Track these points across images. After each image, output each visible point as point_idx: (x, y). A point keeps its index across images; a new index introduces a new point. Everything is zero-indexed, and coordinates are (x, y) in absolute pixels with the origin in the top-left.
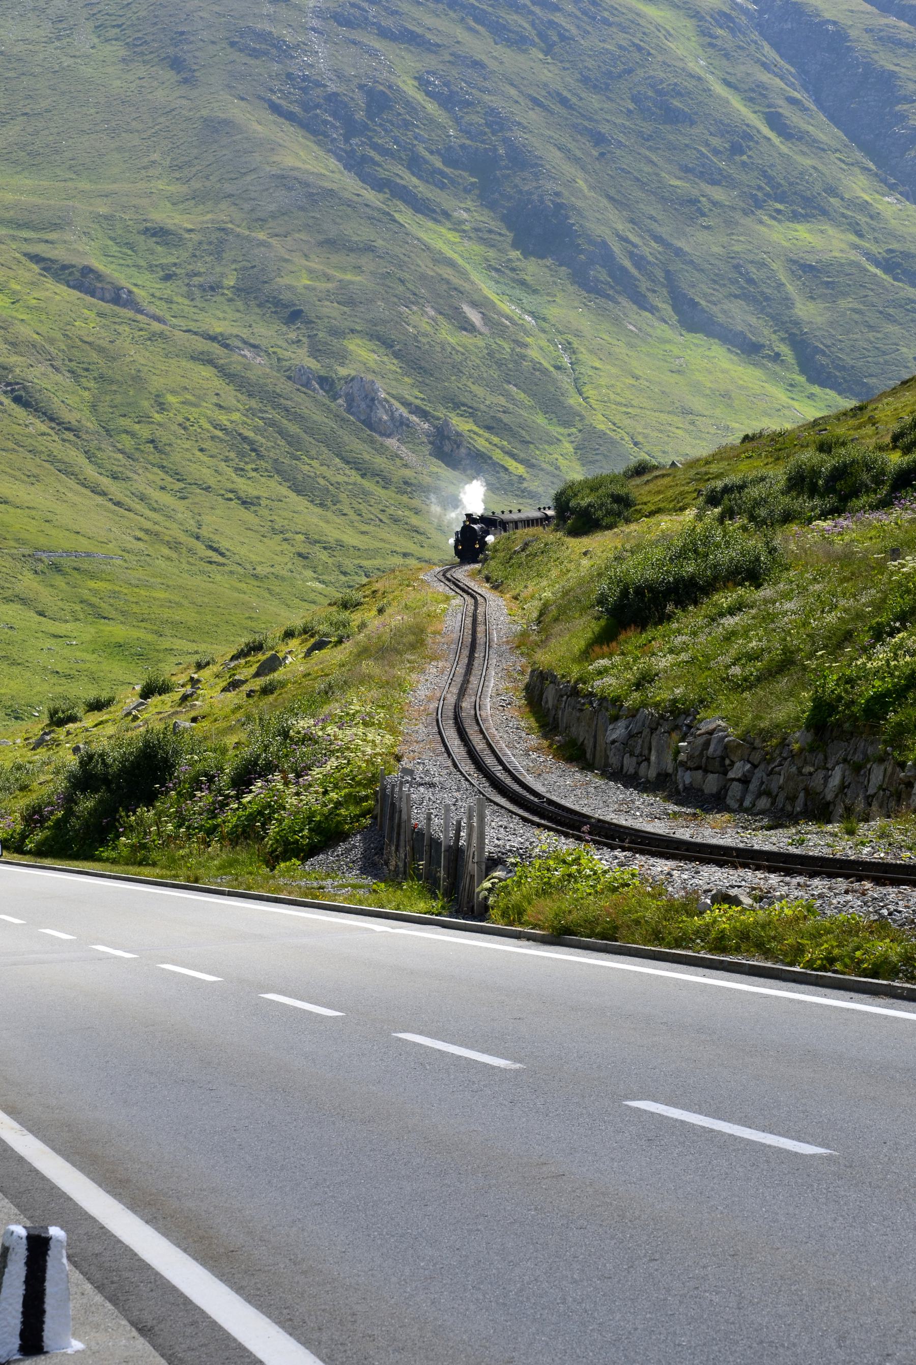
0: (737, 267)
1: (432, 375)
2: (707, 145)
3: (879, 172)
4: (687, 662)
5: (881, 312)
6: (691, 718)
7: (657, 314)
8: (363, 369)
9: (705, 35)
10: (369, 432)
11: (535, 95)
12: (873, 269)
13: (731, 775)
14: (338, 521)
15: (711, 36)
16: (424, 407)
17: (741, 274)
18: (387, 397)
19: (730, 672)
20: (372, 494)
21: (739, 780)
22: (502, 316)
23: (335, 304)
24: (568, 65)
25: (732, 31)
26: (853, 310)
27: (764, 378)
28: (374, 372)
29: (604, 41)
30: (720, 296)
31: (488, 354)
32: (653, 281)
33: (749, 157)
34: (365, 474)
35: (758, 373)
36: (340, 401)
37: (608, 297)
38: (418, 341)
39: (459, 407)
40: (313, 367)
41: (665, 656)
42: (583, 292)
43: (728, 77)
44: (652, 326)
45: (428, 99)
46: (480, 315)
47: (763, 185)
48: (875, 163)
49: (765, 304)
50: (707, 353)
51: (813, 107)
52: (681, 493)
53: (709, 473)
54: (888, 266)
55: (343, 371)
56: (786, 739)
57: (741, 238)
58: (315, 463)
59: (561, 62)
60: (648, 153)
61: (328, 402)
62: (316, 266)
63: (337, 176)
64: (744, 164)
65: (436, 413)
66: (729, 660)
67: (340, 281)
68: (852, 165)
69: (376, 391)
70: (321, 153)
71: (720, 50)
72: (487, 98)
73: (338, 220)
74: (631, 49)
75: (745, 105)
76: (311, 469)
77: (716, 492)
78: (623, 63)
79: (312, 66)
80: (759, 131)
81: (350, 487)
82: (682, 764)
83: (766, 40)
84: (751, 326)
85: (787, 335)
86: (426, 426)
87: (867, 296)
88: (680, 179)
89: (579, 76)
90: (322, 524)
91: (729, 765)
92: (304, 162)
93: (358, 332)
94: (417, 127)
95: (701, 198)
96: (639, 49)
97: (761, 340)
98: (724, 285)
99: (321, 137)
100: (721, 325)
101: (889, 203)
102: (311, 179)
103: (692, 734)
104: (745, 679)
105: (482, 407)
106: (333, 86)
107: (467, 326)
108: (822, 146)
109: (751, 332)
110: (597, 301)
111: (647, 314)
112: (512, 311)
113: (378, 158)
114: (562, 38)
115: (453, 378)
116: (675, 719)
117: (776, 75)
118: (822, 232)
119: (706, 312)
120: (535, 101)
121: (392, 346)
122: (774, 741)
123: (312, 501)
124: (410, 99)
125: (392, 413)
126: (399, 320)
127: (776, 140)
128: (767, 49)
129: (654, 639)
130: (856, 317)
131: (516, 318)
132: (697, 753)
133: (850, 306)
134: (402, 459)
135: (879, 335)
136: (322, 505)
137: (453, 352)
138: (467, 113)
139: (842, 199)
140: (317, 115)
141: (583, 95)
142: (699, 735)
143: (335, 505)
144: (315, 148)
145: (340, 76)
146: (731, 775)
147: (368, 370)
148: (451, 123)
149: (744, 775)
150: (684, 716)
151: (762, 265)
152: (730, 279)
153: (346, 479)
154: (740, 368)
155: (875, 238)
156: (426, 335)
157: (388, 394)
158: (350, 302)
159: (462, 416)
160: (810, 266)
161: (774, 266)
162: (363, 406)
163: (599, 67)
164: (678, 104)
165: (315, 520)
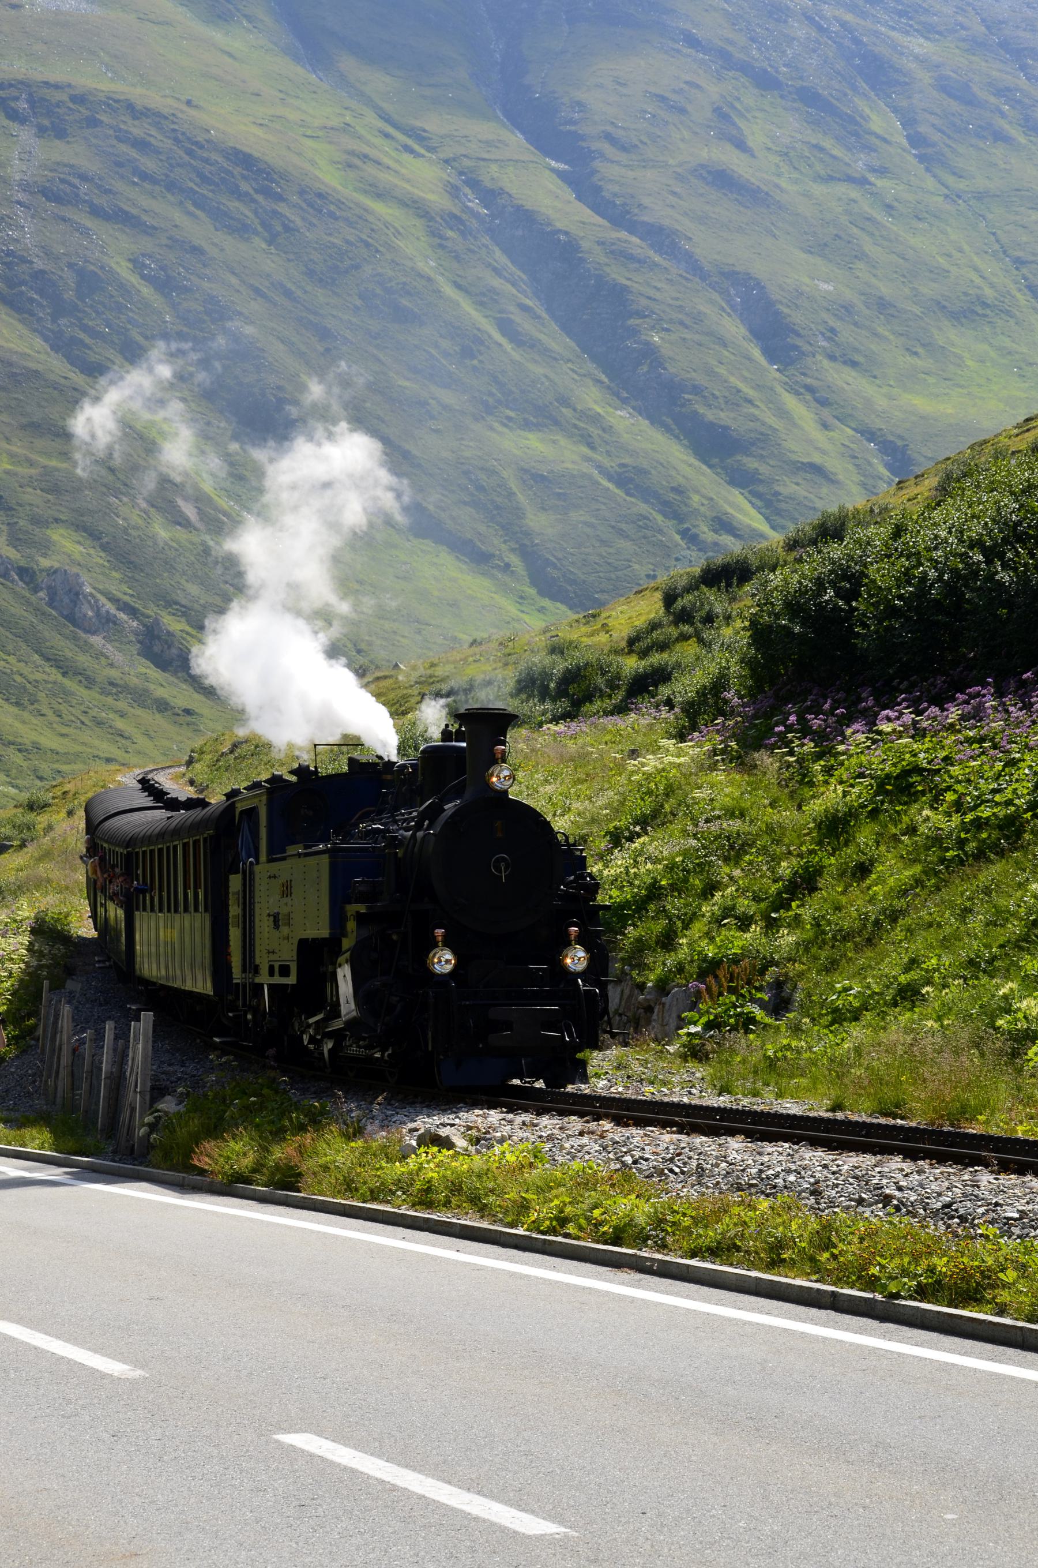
0: (466, 473)
1: (142, 571)
2: (437, 346)
3: (612, 385)
5: (613, 527)
8: (68, 561)
9: (434, 236)
10: (72, 628)
11: (257, 285)
12: (605, 483)
14: (35, 722)
15: (441, 237)
17: (470, 480)
18: (93, 591)
20: (73, 694)
23: (39, 491)
24: (292, 257)
25: (463, 233)
26: (585, 523)
27: (494, 589)
28: (79, 565)
29: (330, 234)
33: (481, 362)
34: (67, 673)
35: (487, 583)
36: (41, 594)
38: (128, 534)
39: (171, 606)
40: (12, 556)
43: (458, 280)
45: (143, 282)
47: (494, 391)
48: (607, 376)
49: (495, 512)
50: (435, 560)
51: (544, 315)
54: (622, 480)
55: (45, 563)
57: (471, 444)
58: (12, 659)
59: (285, 253)
60: (375, 352)
61: (28, 595)
62: (18, 450)
63: (43, 357)
64: (475, 369)
65: (146, 611)
67: (44, 467)
68: (585, 376)
70: (26, 332)
71: (450, 252)
72: (206, 285)
73: (43, 403)
74: (358, 244)
75: (476, 310)
76: (7, 666)
78: (350, 259)
79: (17, 241)
80: (490, 337)
81: (50, 686)
83: (498, 245)
85: (517, 546)
86: (135, 624)
87: (598, 510)
88: (408, 379)
89: (304, 269)
90: (17, 724)
92: (8, 341)
93: (63, 521)
94: (131, 310)
95: (430, 401)
96: (367, 245)
99: (26, 316)
101: (621, 417)
102: (14, 358)
105: (196, 606)
106: (40, 263)
107: (182, 522)
108: (553, 355)
112: (231, 507)
113: (88, 340)
114: (287, 229)
115: (165, 575)
117: (508, 281)
118: (554, 442)
120: (257, 291)
121: (99, 539)
123: (7, 700)
124: (124, 282)
125: (98, 609)
127: (508, 346)
128: (498, 253)
130: (588, 530)
131: (234, 515)
133: (582, 519)
134: (107, 657)
135: (611, 550)
136: (17, 704)
138: (185, 299)
139: (575, 410)
140: (22, 293)
141: (309, 288)
143: (32, 704)
144: (20, 326)
145: (47, 253)
148: (167, 309)
151: (492, 472)
152: (459, 485)
153: (46, 677)
154: (469, 578)
155: (607, 451)
156: (136, 528)
157: (94, 588)
158: (55, 489)
159: (174, 614)
160: (542, 476)
161: (505, 474)
162: (66, 600)
163: (325, 261)
164: (407, 304)
165: (10, 721)
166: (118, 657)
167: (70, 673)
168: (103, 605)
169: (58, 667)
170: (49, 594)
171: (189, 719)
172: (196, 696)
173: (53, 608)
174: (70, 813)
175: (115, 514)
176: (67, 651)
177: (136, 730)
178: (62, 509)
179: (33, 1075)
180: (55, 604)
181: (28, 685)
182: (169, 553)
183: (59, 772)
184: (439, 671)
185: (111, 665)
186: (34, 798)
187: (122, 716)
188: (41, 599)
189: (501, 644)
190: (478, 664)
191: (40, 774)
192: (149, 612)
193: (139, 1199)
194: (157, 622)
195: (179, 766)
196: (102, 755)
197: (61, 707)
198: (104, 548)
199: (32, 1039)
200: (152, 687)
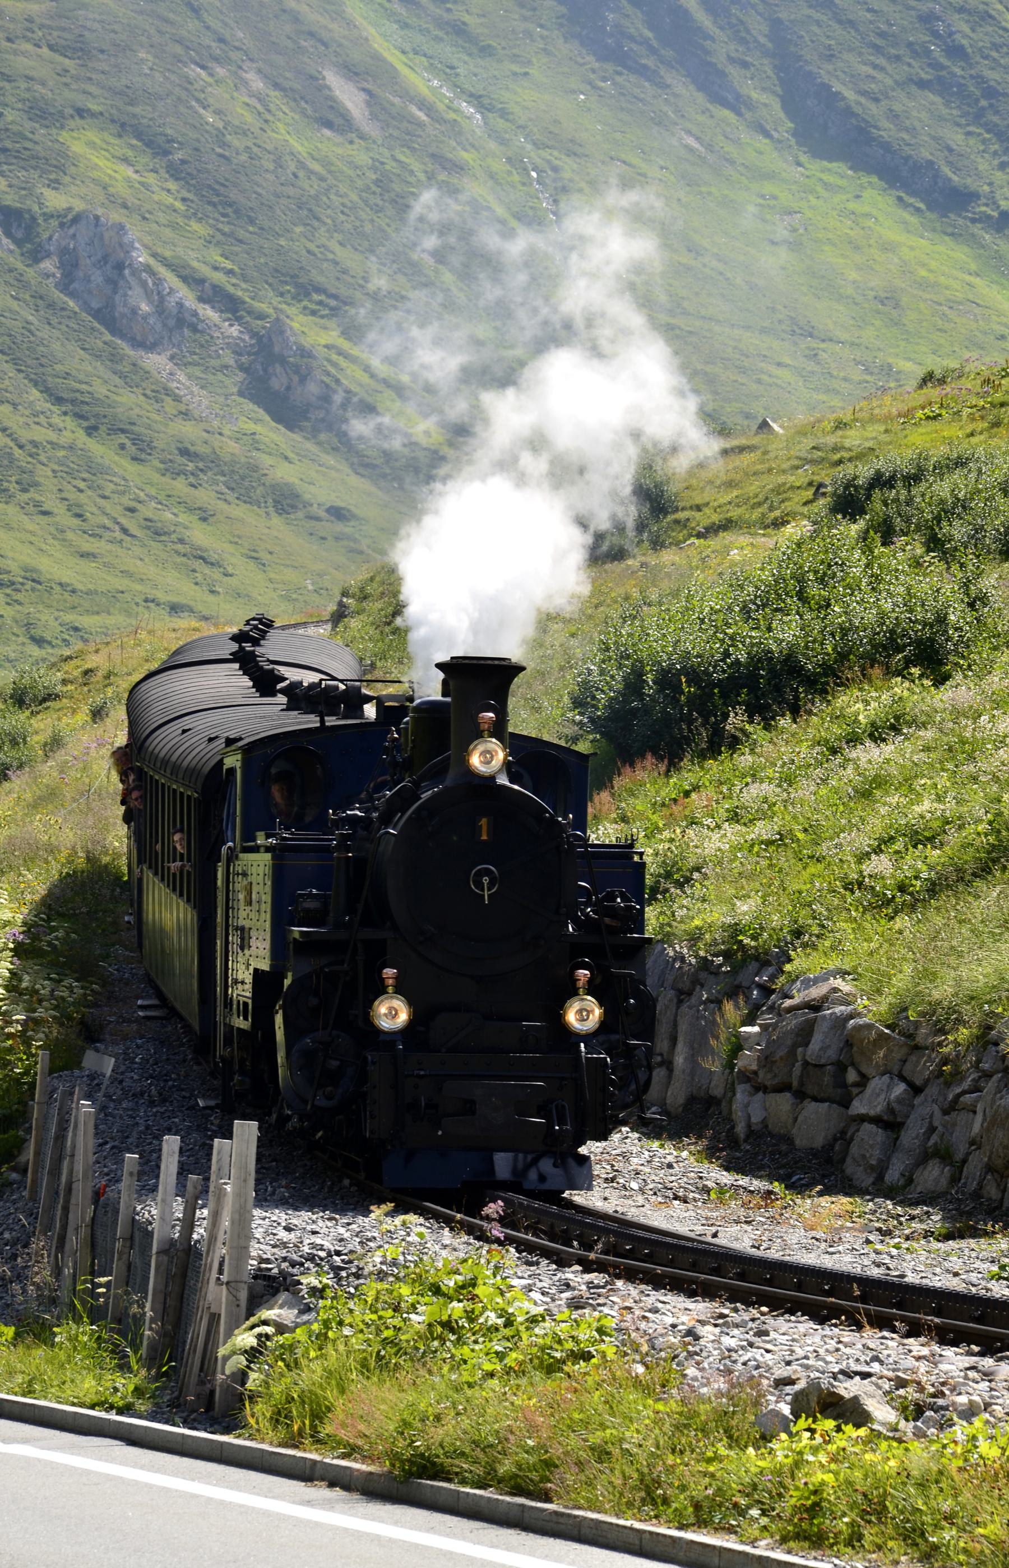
1: (252, 221)
4: (769, 843)
6: (771, 970)
7: (748, 115)
10: (108, 337)
13: (859, 1107)
16: (231, 289)
17: (935, 34)
18: (152, 261)
19: (868, 868)
21: (876, 1120)
22: (412, 100)
27: (973, 267)
28: (125, 206)
30: (889, 82)
31: (377, 182)
32: (743, 41)
34: (95, 428)
35: (962, 253)
37: (643, 71)
38: (224, 145)
41: (718, 827)
42: (590, 58)
44: (737, 142)
46: (363, 96)
49: (984, 103)
52: (778, 490)
53: (843, 448)
56: (990, 1028)
65: (256, 304)
66: (865, 842)
69: (127, 248)
77: (856, 487)
81: (61, 453)
82: (746, 1077)
84: (951, 150)
86: (234, 331)
91: (857, 1085)
97: (972, 184)
98: (898, 58)
100: (886, 147)
103: (771, 1009)
104: (902, 888)
109: (950, 164)
110: (619, 79)
111: (726, 113)
115: (298, 230)
116: (734, 972)
119: (855, 115)
121: (166, 153)
122: (964, 1033)
125: (162, 299)
126: (184, 95)
129: (696, 788)
131: (441, 107)
132: (781, 1053)
134: (177, 399)
137: (301, 174)
142: (791, 1009)
143: (25, 490)
146: (859, 1107)
147: (112, 200)
149: (890, 1110)
150: (754, 966)
152: (910, 45)
153: (53, 436)
157: (154, 255)
162: (97, 277)
166: (200, 400)
167: (103, 428)
168: (172, 291)
169: (79, 416)
170: (62, 265)
171: (340, 527)
172: (354, 480)
173: (72, 295)
174: (97, 714)
175: (198, 100)
176: (97, 383)
177: (231, 548)
178: (92, 89)
179: (13, 1243)
180: (75, 285)
181: (17, 452)
182: (305, 184)
183: (76, 629)
184: (853, 439)
185: (186, 415)
186: (26, 681)
187: (204, 519)
188: (48, 276)
189: (987, 381)
190: (932, 425)
191: (37, 632)
192: (263, 307)
193: (222, 1503)
194: (279, 327)
195: (318, 623)
196: (161, 596)
197: (83, 498)
198: (175, 172)
199: (14, 1169)
200: (266, 461)
